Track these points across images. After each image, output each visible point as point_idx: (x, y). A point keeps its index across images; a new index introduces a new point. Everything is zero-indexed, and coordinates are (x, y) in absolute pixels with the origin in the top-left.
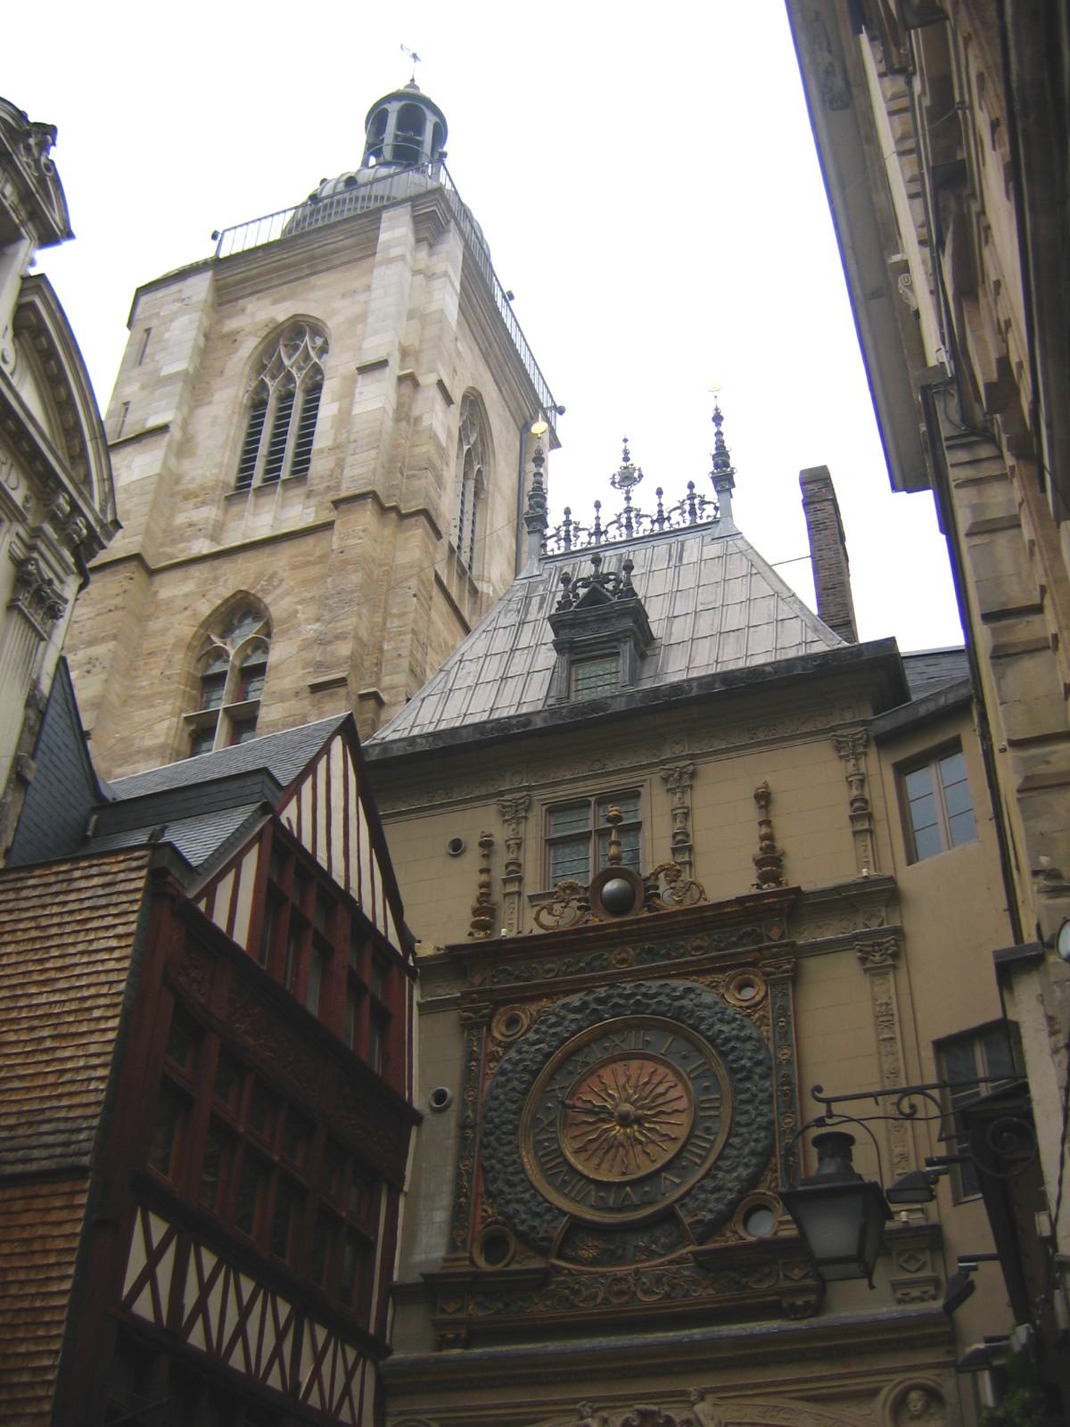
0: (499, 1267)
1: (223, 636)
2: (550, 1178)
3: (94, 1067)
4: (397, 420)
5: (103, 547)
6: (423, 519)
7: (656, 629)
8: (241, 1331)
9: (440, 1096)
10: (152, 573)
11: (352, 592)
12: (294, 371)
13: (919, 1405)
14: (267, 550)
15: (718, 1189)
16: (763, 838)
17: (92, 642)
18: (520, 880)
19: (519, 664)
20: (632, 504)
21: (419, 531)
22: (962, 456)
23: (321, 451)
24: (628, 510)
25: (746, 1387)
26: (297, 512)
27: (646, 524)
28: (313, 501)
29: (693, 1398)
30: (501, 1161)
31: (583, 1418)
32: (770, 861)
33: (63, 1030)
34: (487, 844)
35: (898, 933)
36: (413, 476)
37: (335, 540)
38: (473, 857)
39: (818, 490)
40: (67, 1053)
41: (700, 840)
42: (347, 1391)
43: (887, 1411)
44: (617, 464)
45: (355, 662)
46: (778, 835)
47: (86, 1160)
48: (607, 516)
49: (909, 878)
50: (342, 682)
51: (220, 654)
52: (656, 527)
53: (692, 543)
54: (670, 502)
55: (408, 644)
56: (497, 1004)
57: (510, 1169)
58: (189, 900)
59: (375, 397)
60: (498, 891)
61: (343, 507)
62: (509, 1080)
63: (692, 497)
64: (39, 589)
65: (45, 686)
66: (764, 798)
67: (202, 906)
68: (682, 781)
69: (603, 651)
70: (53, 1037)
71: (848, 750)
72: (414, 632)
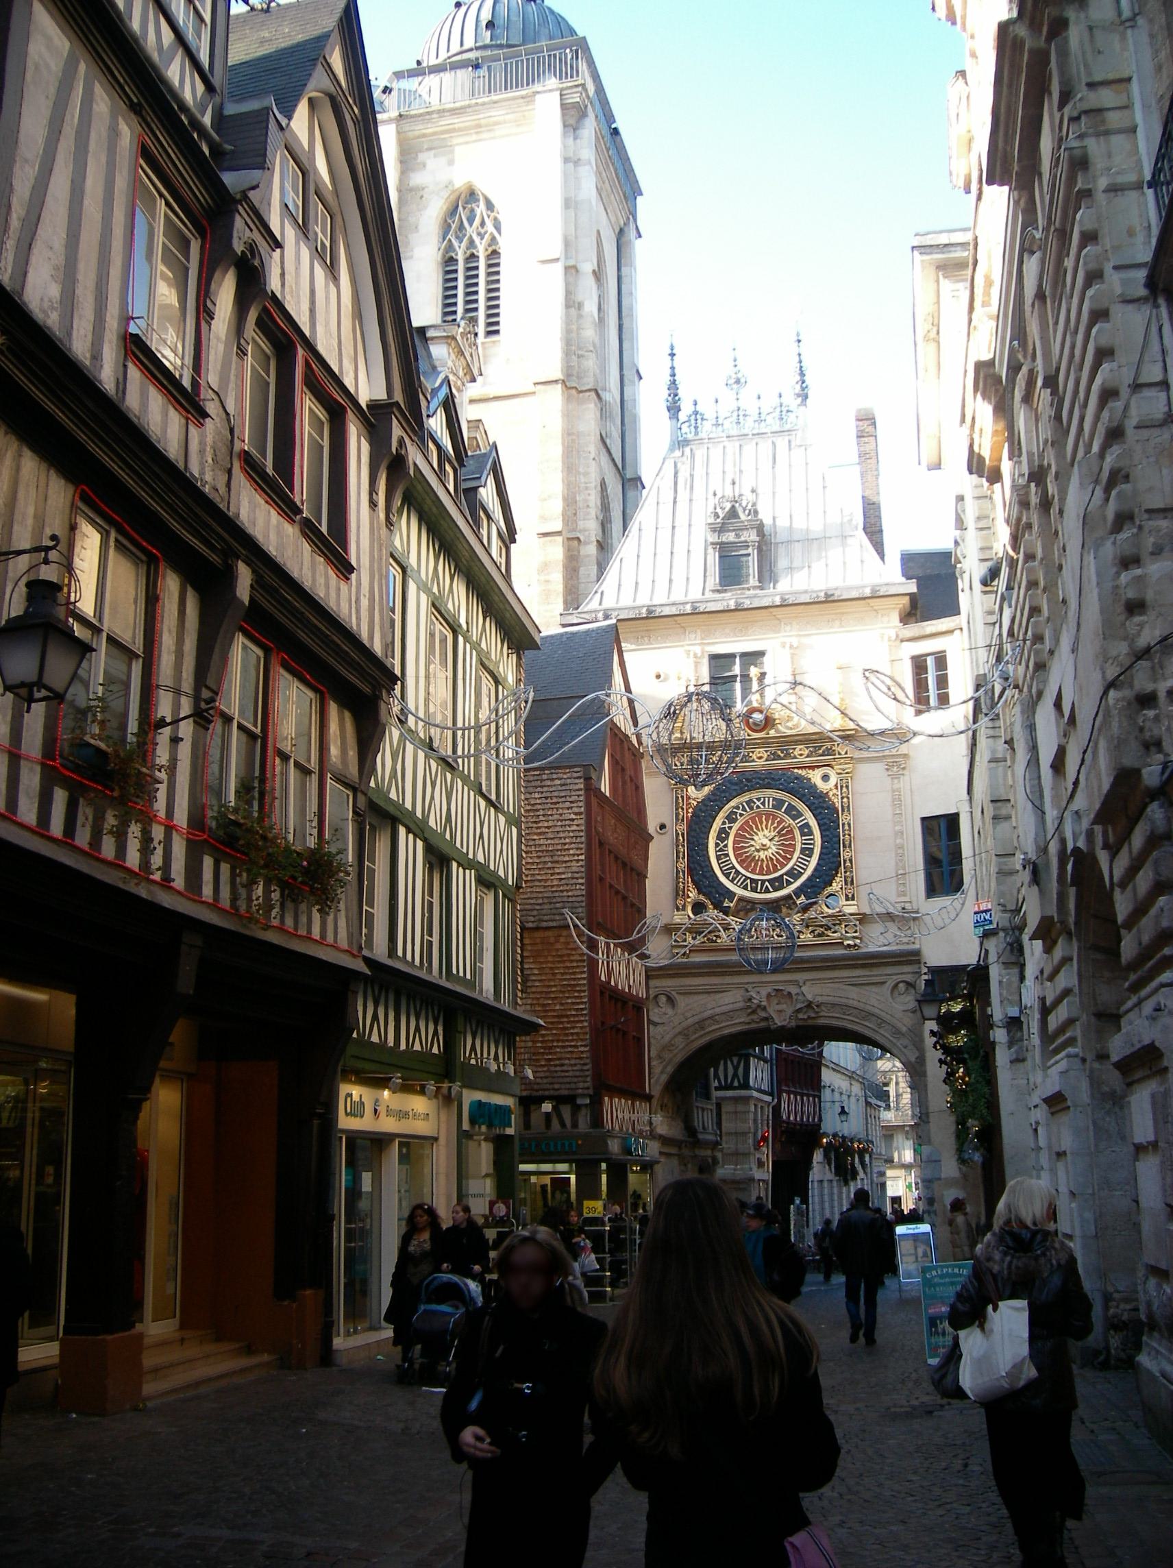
2: (727, 876)
6: (593, 394)
9: (663, 827)
15: (813, 886)
20: (740, 403)
33: (556, 858)
44: (730, 370)
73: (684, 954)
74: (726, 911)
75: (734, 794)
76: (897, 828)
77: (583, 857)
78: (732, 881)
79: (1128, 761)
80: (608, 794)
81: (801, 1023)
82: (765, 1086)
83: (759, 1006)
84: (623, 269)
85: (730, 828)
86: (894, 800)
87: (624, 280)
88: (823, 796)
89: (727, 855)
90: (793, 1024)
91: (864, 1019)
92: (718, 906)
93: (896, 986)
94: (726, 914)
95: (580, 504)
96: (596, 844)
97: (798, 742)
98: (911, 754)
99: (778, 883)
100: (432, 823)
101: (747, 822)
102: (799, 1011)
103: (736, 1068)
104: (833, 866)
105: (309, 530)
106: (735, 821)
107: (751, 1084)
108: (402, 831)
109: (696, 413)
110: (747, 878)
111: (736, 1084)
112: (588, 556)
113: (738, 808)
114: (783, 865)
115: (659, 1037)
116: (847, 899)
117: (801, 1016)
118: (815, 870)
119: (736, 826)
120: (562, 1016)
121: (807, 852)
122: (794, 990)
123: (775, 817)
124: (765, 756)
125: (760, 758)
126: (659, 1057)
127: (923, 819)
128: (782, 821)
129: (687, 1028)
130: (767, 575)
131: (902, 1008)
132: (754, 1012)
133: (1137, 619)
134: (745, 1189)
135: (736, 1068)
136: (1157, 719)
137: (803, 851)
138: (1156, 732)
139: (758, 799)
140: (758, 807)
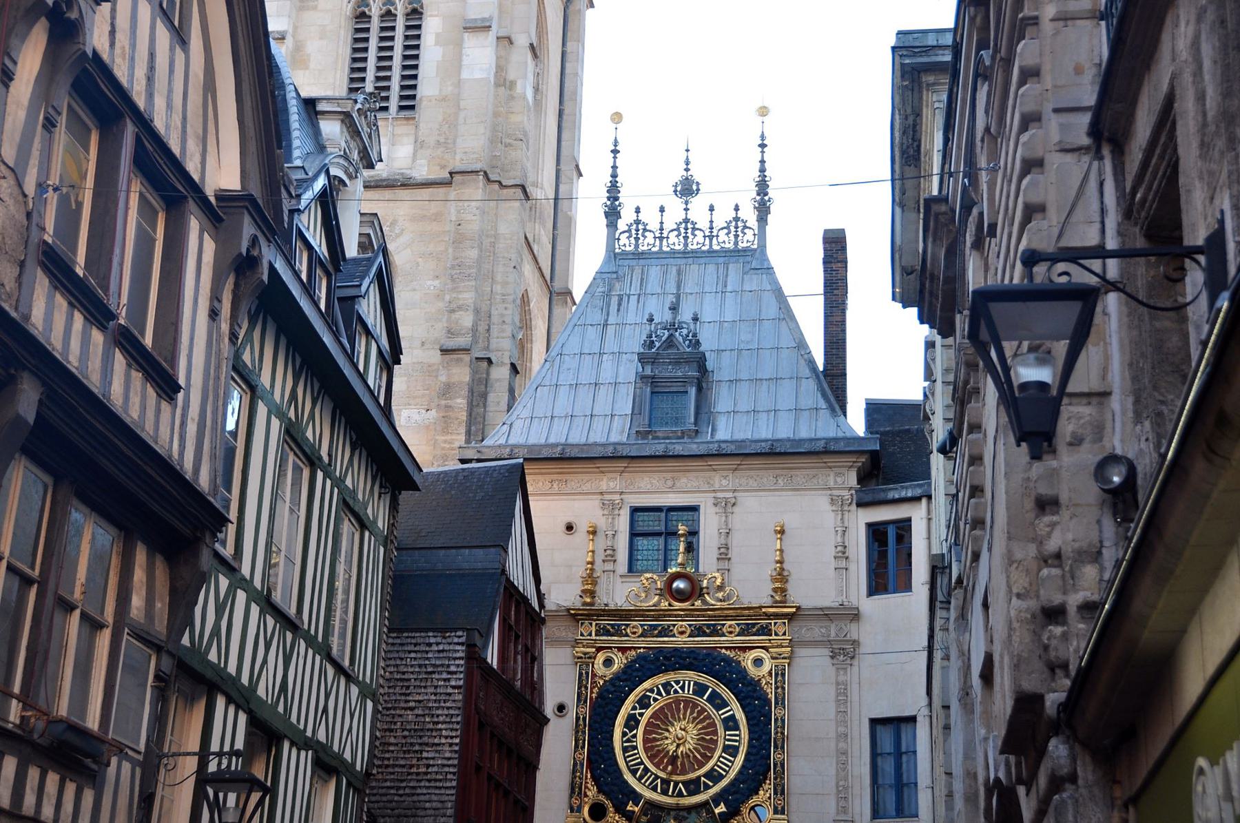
2: (634, 772)
3: (449, 766)
4: (497, 85)
6: (519, 191)
9: (561, 708)
11: (470, 267)
24: (686, 221)
32: (781, 577)
33: (425, 740)
35: (856, 643)
36: (510, 145)
38: (581, 535)
41: (733, 554)
44: (678, 174)
45: (474, 330)
50: (466, 350)
53: (734, 270)
54: (719, 222)
56: (599, 649)
59: (479, 56)
60: (599, 566)
63: (737, 219)
68: (726, 506)
70: (420, 744)
75: (649, 673)
76: (841, 729)
77: (457, 741)
78: (639, 780)
79: (1029, 685)
80: (495, 665)
84: (569, 44)
85: (641, 715)
86: (838, 695)
87: (569, 57)
88: (755, 684)
89: (635, 748)
92: (620, 809)
95: (495, 319)
96: (476, 724)
97: (726, 618)
98: (861, 640)
99: (694, 787)
100: (261, 692)
101: (662, 708)
104: (762, 769)
105: (127, 341)
106: (647, 706)
108: (220, 702)
109: (638, 222)
112: (497, 380)
113: (652, 691)
114: (701, 765)
116: (776, 812)
118: (740, 772)
119: (648, 713)
121: (732, 751)
124: (689, 632)
125: (682, 633)
127: (874, 722)
130: (704, 417)
133: (1047, 519)
136: (1065, 637)
137: (726, 749)
138: (1062, 654)
139: (677, 682)
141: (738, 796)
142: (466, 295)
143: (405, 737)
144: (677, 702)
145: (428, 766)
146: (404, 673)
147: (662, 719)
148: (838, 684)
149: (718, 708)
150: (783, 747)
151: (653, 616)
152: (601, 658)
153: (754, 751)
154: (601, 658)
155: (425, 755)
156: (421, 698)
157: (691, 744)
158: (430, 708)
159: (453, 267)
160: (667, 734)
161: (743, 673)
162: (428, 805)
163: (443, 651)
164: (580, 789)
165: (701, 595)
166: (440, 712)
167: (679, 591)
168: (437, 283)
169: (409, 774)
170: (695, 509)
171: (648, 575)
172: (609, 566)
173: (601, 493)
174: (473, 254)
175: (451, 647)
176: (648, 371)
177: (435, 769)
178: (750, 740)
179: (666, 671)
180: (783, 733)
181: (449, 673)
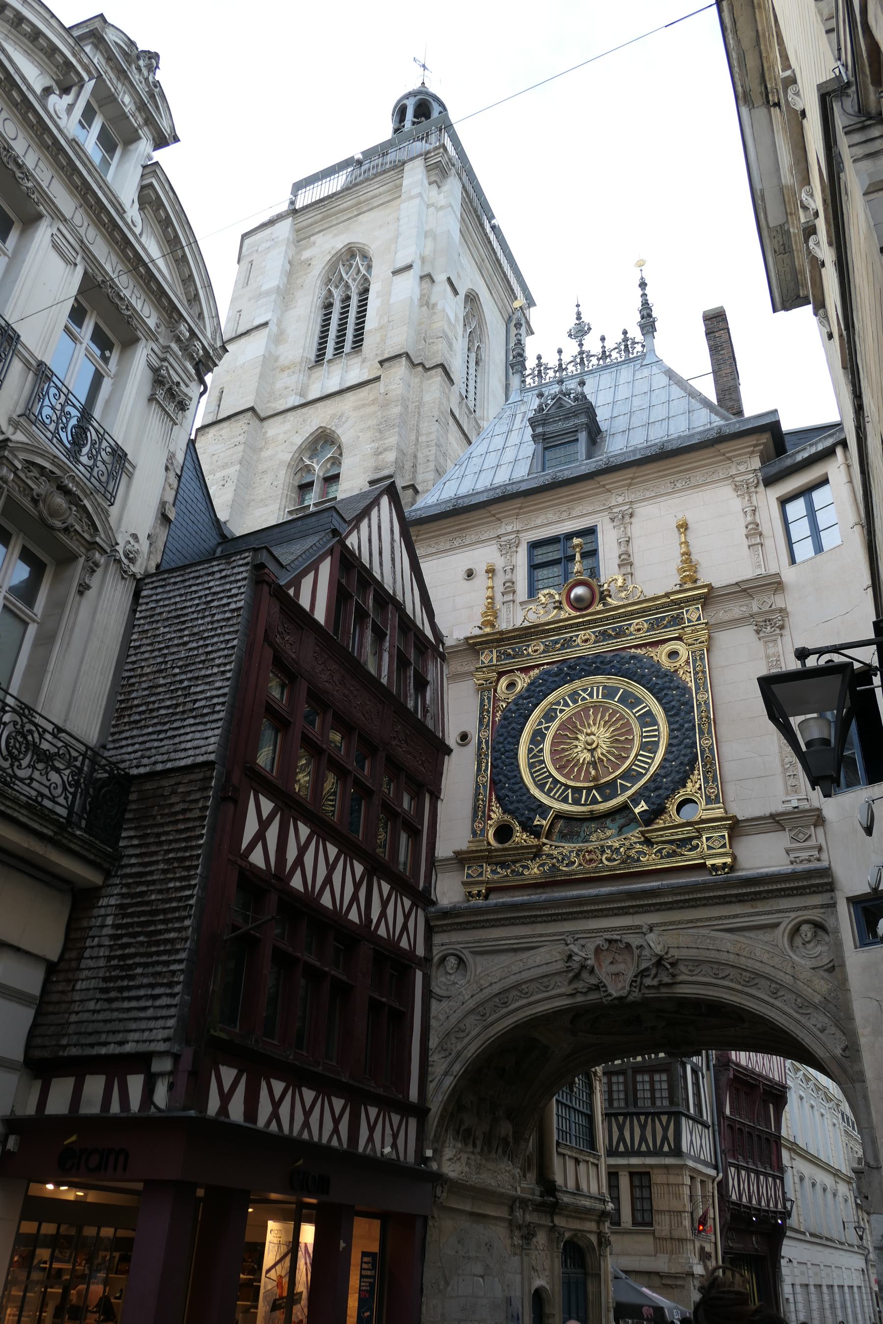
0: (506, 845)
1: (310, 458)
2: (541, 787)
3: (218, 696)
5: (216, 365)
6: (440, 370)
7: (603, 426)
8: (328, 880)
9: (464, 737)
10: (262, 420)
12: (350, 281)
13: (809, 935)
14: (337, 398)
15: (657, 788)
16: (683, 554)
17: (225, 466)
18: (514, 592)
19: (509, 455)
21: (437, 377)
22: (857, 138)
23: (370, 331)
24: (581, 353)
25: (680, 922)
26: (354, 370)
27: (594, 361)
28: (367, 364)
29: (644, 930)
30: (505, 776)
31: (567, 945)
34: (491, 571)
37: (381, 386)
38: (481, 579)
39: (716, 323)
40: (199, 689)
41: (636, 559)
42: (405, 927)
43: (786, 939)
46: (693, 550)
47: (212, 757)
48: (566, 358)
49: (789, 575)
51: (308, 469)
52: (601, 362)
54: (610, 344)
55: (433, 452)
57: (512, 781)
58: (280, 586)
60: (499, 598)
61: (386, 365)
62: (509, 724)
63: (626, 340)
64: (170, 389)
65: (180, 457)
66: (683, 527)
67: (291, 592)
68: (625, 518)
69: (568, 439)
71: (743, 489)
72: (438, 445)
73: (479, 894)
74: (536, 832)
78: (548, 794)
81: (651, 994)
82: (707, 1154)
83: (583, 967)
85: (547, 728)
89: (543, 762)
90: (636, 995)
91: (747, 983)
92: (527, 827)
93: (796, 931)
94: (538, 836)
97: (632, 615)
98: (789, 609)
101: (570, 718)
102: (643, 973)
103: (665, 1129)
104: (686, 760)
107: (684, 1149)
110: (567, 787)
111: (666, 1148)
115: (442, 1017)
117: (648, 981)
118: (661, 766)
119: (555, 725)
120: (157, 912)
121: (650, 747)
122: (635, 940)
123: (606, 709)
126: (441, 1047)
128: (615, 712)
129: (482, 1004)
131: (809, 964)
132: (577, 977)
134: (683, 1287)
135: (665, 1129)
137: (643, 746)
139: (585, 690)
140: (584, 699)
141: (661, 792)
142: (391, 440)
143: (175, 675)
144: (586, 709)
145: (195, 701)
146: (182, 609)
147: (570, 729)
148: (768, 657)
149: (632, 706)
150: (709, 732)
151: (553, 630)
152: (503, 683)
153: (675, 741)
154: (503, 683)
155: (193, 690)
156: (196, 630)
157: (604, 747)
158: (205, 639)
159: (381, 423)
160: (576, 743)
161: (656, 667)
162: (189, 745)
163: (225, 577)
164: (484, 812)
165: (603, 598)
166: (215, 640)
167: (579, 599)
168: (372, 445)
169: (173, 714)
170: (590, 532)
171: (546, 591)
172: (509, 597)
173: (499, 537)
174: (397, 410)
175: (235, 571)
176: (540, 430)
177: (203, 703)
178: (672, 730)
179: (572, 680)
180: (708, 717)
181: (229, 597)
